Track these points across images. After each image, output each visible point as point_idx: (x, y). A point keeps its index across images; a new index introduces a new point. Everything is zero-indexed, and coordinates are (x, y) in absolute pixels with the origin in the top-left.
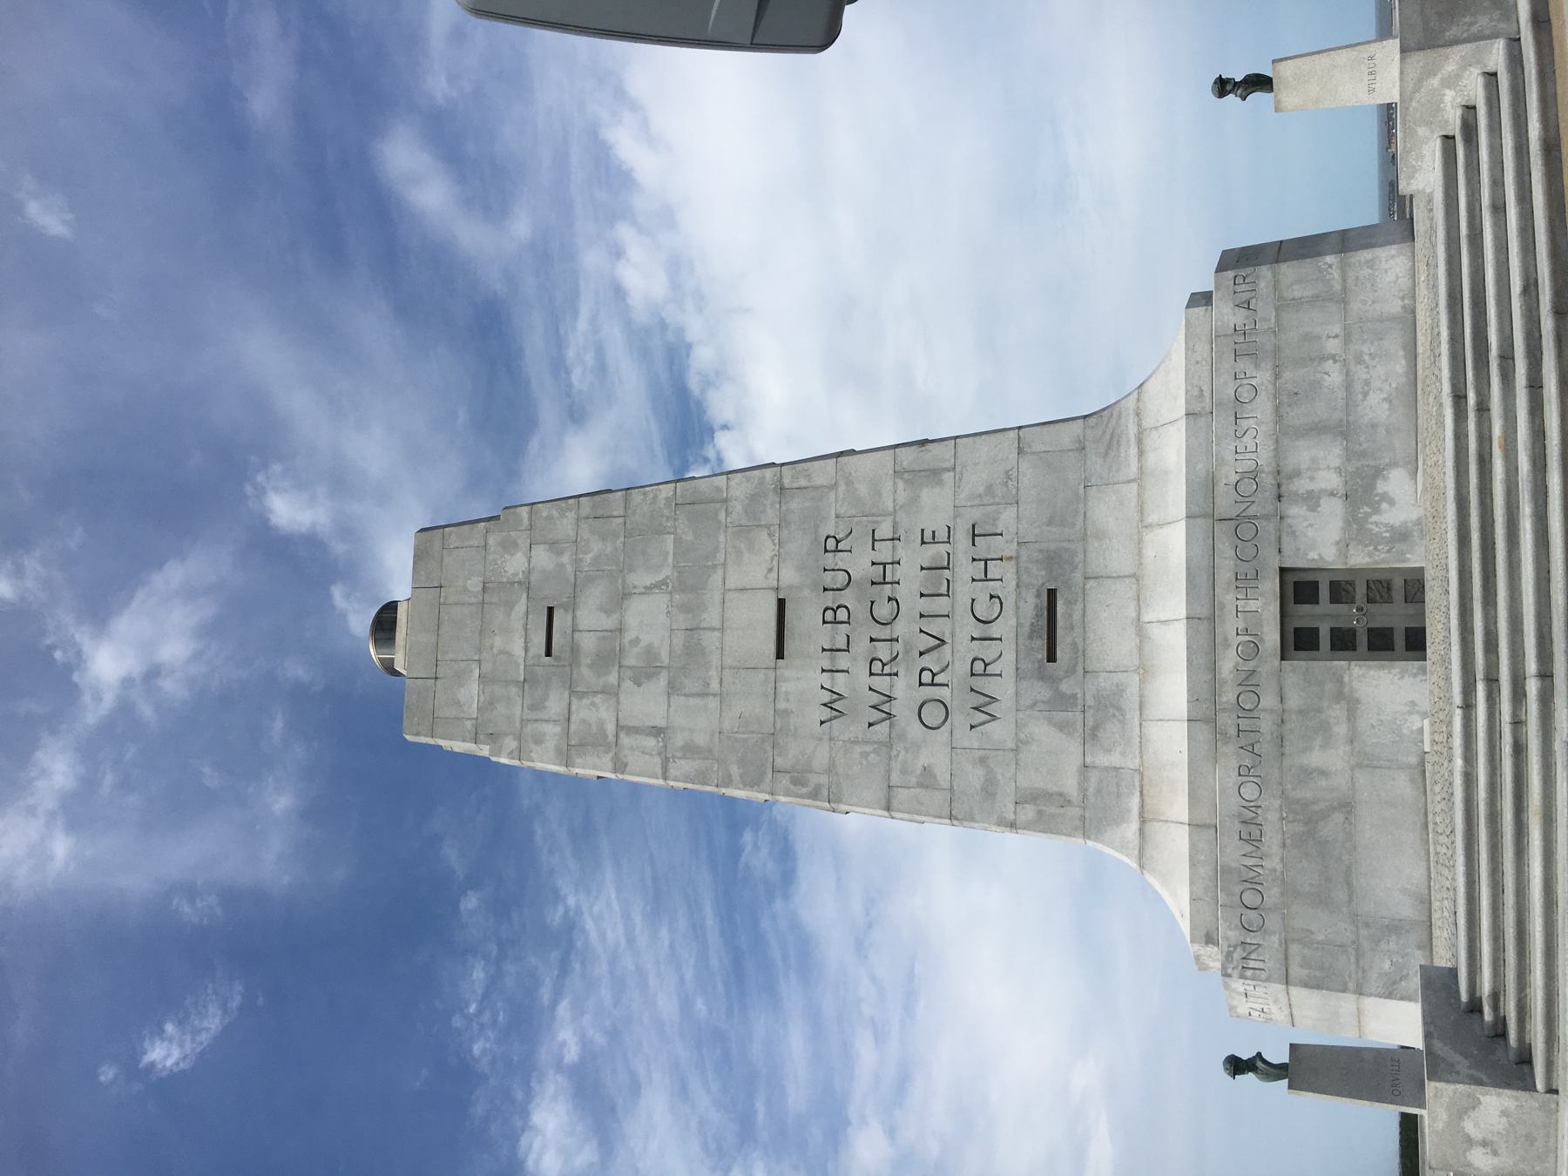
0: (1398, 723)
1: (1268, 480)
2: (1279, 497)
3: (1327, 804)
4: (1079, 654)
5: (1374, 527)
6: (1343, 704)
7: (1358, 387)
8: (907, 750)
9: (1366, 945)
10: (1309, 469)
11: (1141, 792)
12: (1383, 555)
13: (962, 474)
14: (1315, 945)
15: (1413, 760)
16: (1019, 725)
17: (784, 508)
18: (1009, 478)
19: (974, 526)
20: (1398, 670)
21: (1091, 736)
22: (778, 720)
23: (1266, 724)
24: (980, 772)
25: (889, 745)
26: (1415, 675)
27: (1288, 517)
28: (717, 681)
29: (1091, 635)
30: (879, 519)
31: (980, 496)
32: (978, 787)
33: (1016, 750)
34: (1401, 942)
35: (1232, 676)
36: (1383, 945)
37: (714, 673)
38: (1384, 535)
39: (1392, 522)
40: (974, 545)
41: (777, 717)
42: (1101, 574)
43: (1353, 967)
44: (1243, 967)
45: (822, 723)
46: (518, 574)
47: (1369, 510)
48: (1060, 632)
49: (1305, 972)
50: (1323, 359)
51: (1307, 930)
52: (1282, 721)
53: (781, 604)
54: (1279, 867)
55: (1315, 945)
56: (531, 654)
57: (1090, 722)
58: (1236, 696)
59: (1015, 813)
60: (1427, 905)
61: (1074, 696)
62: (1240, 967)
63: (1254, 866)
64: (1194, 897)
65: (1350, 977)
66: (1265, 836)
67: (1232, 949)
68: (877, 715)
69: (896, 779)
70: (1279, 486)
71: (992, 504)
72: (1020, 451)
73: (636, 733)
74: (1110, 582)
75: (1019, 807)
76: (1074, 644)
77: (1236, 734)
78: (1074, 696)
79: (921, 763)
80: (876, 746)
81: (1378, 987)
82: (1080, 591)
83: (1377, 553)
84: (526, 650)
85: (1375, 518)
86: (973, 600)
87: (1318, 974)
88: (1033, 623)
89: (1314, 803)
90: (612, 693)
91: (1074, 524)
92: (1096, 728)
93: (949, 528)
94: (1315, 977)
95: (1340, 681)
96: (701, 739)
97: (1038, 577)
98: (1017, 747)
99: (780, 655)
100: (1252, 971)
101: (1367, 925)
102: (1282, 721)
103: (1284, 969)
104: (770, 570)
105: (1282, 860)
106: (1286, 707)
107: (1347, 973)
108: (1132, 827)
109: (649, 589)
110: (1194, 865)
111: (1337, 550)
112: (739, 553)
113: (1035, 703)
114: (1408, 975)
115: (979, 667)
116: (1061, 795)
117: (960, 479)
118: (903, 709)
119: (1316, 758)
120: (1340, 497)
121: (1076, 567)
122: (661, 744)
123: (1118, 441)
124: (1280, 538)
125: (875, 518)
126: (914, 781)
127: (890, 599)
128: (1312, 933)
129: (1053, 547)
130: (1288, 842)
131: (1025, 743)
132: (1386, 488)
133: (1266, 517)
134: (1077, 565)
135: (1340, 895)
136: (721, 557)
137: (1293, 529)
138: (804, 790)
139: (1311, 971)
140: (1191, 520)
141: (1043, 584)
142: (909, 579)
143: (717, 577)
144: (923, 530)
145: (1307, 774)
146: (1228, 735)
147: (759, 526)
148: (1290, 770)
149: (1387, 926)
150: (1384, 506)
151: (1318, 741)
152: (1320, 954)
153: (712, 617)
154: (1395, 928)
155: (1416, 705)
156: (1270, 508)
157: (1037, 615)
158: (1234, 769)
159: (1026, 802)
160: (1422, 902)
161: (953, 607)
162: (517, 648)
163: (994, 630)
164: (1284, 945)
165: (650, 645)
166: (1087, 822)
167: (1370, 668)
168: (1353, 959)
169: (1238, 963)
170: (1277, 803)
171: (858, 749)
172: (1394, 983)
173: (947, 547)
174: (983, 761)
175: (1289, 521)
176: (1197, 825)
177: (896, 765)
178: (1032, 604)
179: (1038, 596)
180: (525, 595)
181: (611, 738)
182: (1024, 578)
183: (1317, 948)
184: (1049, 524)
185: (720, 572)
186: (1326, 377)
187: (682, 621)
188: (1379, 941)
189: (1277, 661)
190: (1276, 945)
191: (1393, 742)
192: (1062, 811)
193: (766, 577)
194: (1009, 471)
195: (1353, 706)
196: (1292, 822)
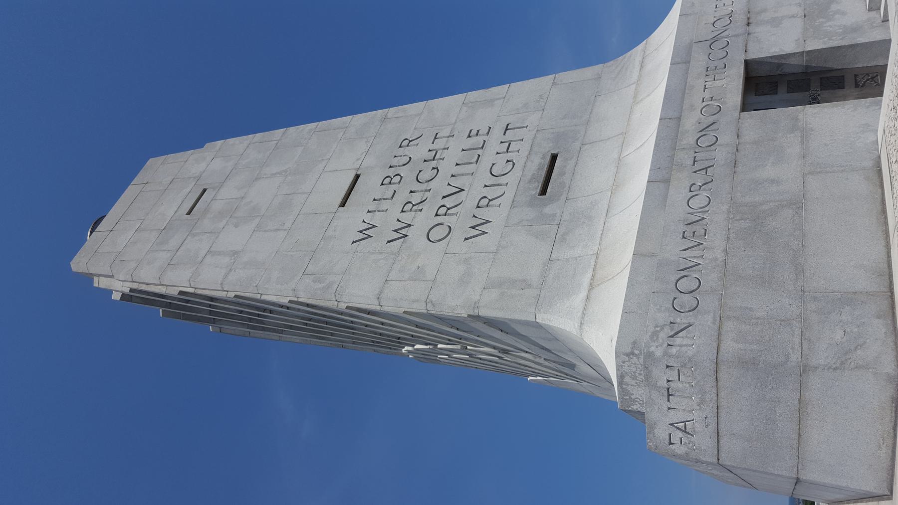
1: (740, 18)
2: (748, 24)
4: (565, 189)
11: (594, 269)
12: (836, 42)
13: (509, 99)
14: (754, 321)
15: (869, 164)
17: (382, 128)
18: (541, 97)
19: (508, 125)
23: (721, 155)
26: (868, 107)
27: (755, 33)
28: (291, 222)
30: (443, 127)
33: (496, 253)
35: (693, 127)
38: (837, 31)
40: (504, 134)
41: (322, 242)
44: (669, 345)
45: (354, 242)
47: (824, 20)
49: (741, 346)
51: (746, 308)
53: (357, 177)
54: (720, 256)
55: (754, 321)
56: (177, 214)
57: (562, 230)
60: (887, 277)
61: (554, 215)
62: (666, 345)
63: (695, 257)
64: (626, 311)
65: (793, 348)
66: (708, 233)
67: (658, 329)
68: (397, 235)
70: (748, 19)
71: (526, 112)
72: (554, 84)
77: (692, 163)
78: (554, 215)
83: (831, 41)
85: (828, 24)
86: (493, 164)
87: (755, 347)
88: (535, 174)
89: (761, 204)
93: (490, 128)
95: (796, 119)
97: (548, 148)
98: (498, 250)
99: (343, 204)
101: (815, 299)
102: (737, 150)
105: (725, 250)
107: (790, 345)
108: (583, 294)
109: (274, 175)
110: (632, 285)
111: (796, 44)
114: (865, 343)
115: (484, 202)
116: (524, 281)
118: (416, 234)
120: (800, 17)
121: (577, 139)
122: (232, 261)
123: (627, 69)
124: (746, 44)
125: (441, 127)
127: (433, 168)
128: (751, 309)
130: (731, 236)
132: (839, 8)
133: (737, 36)
139: (747, 345)
140: (674, 66)
141: (549, 151)
142: (453, 154)
144: (471, 131)
150: (837, 16)
154: (849, 299)
157: (539, 169)
158: (685, 188)
159: (492, 287)
161: (476, 170)
163: (503, 180)
166: (541, 299)
168: (797, 332)
169: (663, 341)
170: (724, 208)
172: (846, 353)
173: (485, 138)
175: (755, 35)
178: (538, 163)
179: (544, 157)
180: (194, 183)
181: (200, 259)
183: (757, 323)
185: (324, 163)
189: (737, 113)
191: (846, 153)
192: (521, 292)
193: (354, 163)
194: (542, 95)
195: (805, 134)
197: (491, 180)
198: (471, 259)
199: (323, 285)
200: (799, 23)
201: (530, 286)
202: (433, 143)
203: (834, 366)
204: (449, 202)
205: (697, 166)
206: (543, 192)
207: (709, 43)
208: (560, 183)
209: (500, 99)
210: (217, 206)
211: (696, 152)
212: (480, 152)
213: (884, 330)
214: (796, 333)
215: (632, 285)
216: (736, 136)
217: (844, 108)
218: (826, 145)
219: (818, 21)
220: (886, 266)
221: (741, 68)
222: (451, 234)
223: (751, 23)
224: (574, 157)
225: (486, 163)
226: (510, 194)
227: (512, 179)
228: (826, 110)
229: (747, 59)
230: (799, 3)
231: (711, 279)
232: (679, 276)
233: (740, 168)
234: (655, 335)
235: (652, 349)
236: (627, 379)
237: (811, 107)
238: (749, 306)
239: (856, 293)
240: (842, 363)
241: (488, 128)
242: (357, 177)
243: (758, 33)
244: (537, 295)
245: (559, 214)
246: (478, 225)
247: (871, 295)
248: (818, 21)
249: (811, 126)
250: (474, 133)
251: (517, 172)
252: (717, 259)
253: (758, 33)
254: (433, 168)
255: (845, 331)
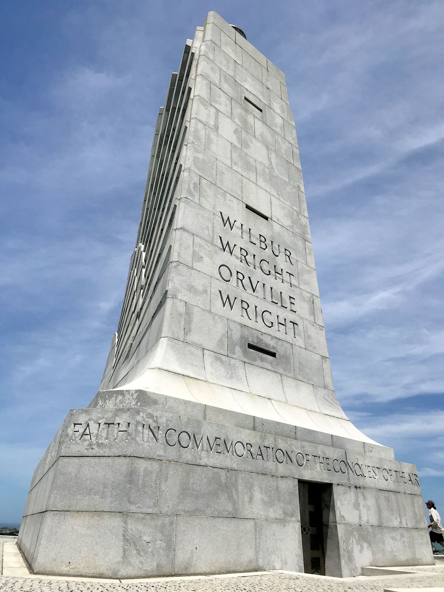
0: (277, 552)
1: (360, 482)
2: (356, 487)
3: (236, 500)
4: (251, 361)
5: (351, 541)
6: (282, 517)
7: (394, 534)
8: (210, 251)
9: (159, 522)
10: (367, 504)
12: (342, 545)
13: (314, 326)
15: (261, 563)
16: (222, 318)
17: (299, 238)
19: (297, 324)
20: (299, 554)
21: (217, 356)
22: (222, 191)
23: (270, 465)
24: (200, 288)
25: (212, 243)
26: (298, 564)
27: (350, 491)
28: (237, 170)
29: (260, 370)
30: (297, 280)
31: (307, 332)
32: (193, 284)
33: (210, 312)
34: (161, 551)
36: (159, 536)
37: (239, 170)
38: (349, 547)
39: (354, 551)
40: (290, 322)
42: (283, 384)
43: (145, 510)
44: (144, 425)
45: (221, 213)
46: (273, 105)
48: (261, 354)
49: (142, 473)
50: (400, 517)
51: (167, 477)
52: (273, 476)
53: (266, 218)
54: (203, 462)
55: (158, 482)
57: (223, 358)
58: (282, 449)
59: (181, 300)
61: (234, 353)
63: (203, 445)
64: (167, 398)
65: (139, 507)
67: (155, 418)
68: (225, 243)
69: (197, 240)
70: (360, 487)
72: (323, 357)
73: (215, 117)
74: (281, 387)
75: (184, 304)
76: (255, 359)
77: (266, 446)
78: (234, 353)
79: (204, 257)
80: (212, 236)
81: (132, 530)
82: (275, 370)
83: (343, 542)
84: (246, 89)
85: (354, 540)
86: (270, 313)
87: (141, 482)
90: (231, 116)
91: (300, 374)
92: (221, 361)
94: (138, 479)
95: (292, 516)
96: (213, 147)
97: (280, 350)
99: (248, 207)
100: (142, 431)
101: (171, 523)
102: (273, 476)
103: (143, 456)
104: (278, 219)
106: (279, 479)
107: (141, 506)
109: (270, 159)
110: (185, 403)
112: (284, 208)
113: (231, 330)
114: (141, 556)
115: (245, 306)
116: (190, 331)
117: (312, 324)
118: (225, 257)
119: (258, 495)
121: (284, 371)
122: (211, 126)
125: (297, 278)
126: (196, 249)
127: (270, 272)
128: (166, 480)
129: (292, 361)
131: (213, 318)
132: (365, 548)
133: (349, 479)
134: (286, 372)
135: (188, 505)
136: (282, 199)
137: (346, 493)
138: (192, 188)
141: (278, 352)
143: (275, 193)
144: (294, 299)
145: (250, 488)
146: (264, 440)
147: (293, 224)
148: (251, 478)
149: (171, 540)
150: (359, 547)
151: (266, 499)
152: (153, 485)
153: (261, 182)
155: (286, 565)
156: (352, 482)
157: (266, 344)
159: (186, 308)
160: (186, 568)
162: (247, 86)
163: (259, 319)
164: (157, 458)
165: (249, 146)
166: (176, 341)
167: (299, 535)
168: (150, 511)
171: (210, 226)
172: (134, 543)
173: (289, 309)
174: (205, 291)
175: (349, 491)
176: (205, 410)
177: (203, 242)
178: (269, 343)
179: (274, 348)
180: (266, 103)
181: (213, 104)
182: (280, 343)
184: (300, 363)
186: (395, 518)
187: (259, 168)
188: (162, 533)
190: (158, 452)
192: (182, 328)
193: (276, 216)
195: (282, 521)
196: (227, 477)
197: (260, 310)
198: (207, 294)
199: (192, 189)
200: (356, 521)
201: (186, 334)
202: (287, 272)
203: (126, 535)
204: (246, 281)
205: (263, 449)
206: (251, 346)
207: (345, 460)
208: (256, 358)
209: (314, 320)
210: (250, 119)
211: (273, 448)
212: (279, 304)
213: (148, 569)
214: (149, 510)
215: (185, 403)
216: (282, 476)
217: (298, 548)
218: (274, 535)
219: (356, 534)
220: (192, 572)
221: (328, 481)
222: (225, 282)
223: (357, 489)
224: (273, 369)
225: (272, 308)
226: (250, 323)
227: (260, 326)
228: (297, 536)
229: (333, 485)
230: (369, 522)
231: (187, 455)
232: (190, 434)
233: (261, 477)
234: (151, 416)
235: (141, 414)
236: (120, 397)
237: (299, 526)
238: (168, 479)
239: (175, 551)
240: (127, 540)
241: (295, 311)
242: (266, 218)
243: (350, 493)
244: (180, 339)
245: (234, 356)
246: (229, 301)
247: (172, 561)
248: (356, 534)
249: (287, 526)
250: (293, 301)
251: (265, 330)
252: (200, 459)
253: (350, 493)
254: (270, 272)
255: (149, 542)
